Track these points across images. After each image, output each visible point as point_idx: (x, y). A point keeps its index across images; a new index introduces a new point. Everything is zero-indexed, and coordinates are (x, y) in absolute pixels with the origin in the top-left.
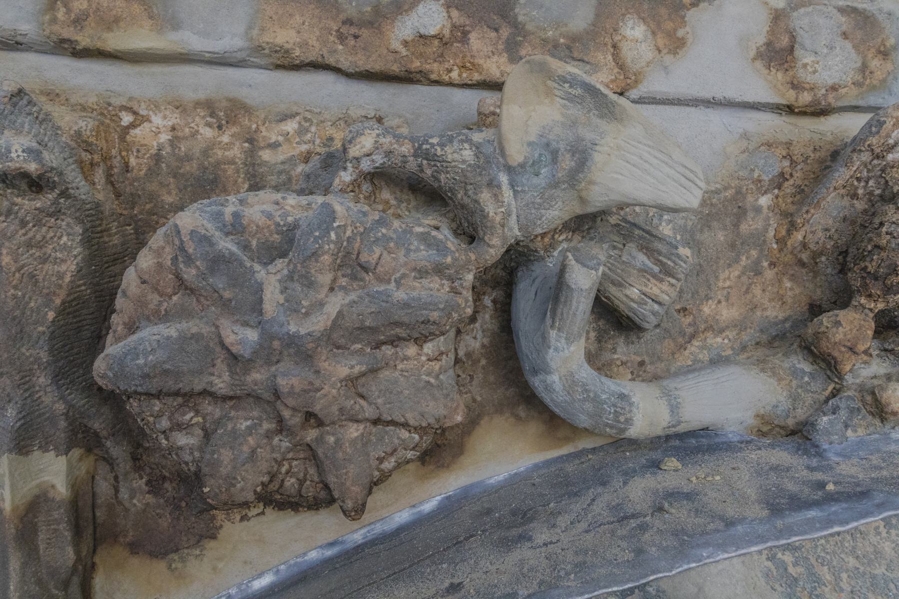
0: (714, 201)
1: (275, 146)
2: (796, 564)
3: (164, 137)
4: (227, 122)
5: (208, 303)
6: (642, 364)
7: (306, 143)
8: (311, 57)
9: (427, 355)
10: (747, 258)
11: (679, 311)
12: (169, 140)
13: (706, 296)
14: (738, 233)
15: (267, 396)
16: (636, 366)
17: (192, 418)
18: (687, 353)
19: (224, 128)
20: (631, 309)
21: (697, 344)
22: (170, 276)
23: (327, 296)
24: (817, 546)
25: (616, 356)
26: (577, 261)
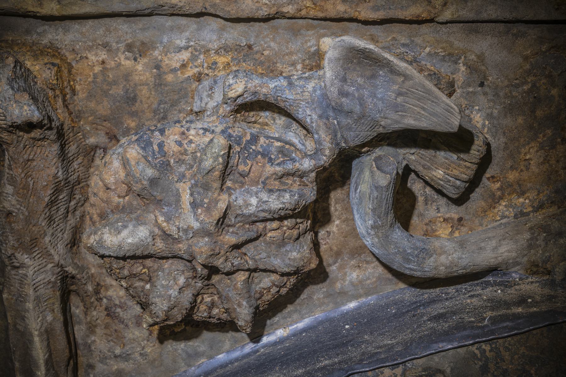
0: (514, 93)
1: (174, 71)
2: (490, 351)
3: (97, 69)
4: (140, 56)
5: (148, 202)
6: (460, 219)
7: (196, 67)
8: (198, 9)
9: (286, 226)
10: (544, 136)
11: (488, 179)
12: (101, 71)
13: (511, 167)
14: (536, 117)
15: (186, 256)
16: (456, 222)
17: (142, 270)
18: (496, 210)
19: (138, 60)
20: (439, 185)
21: (504, 204)
22: (124, 185)
23: (219, 195)
24: (506, 341)
25: (439, 215)
26: (378, 168)
